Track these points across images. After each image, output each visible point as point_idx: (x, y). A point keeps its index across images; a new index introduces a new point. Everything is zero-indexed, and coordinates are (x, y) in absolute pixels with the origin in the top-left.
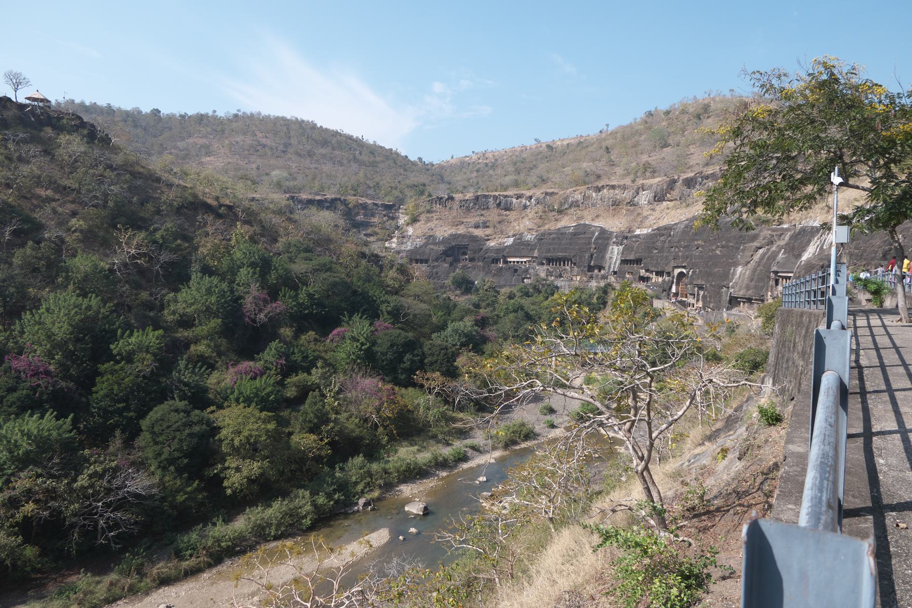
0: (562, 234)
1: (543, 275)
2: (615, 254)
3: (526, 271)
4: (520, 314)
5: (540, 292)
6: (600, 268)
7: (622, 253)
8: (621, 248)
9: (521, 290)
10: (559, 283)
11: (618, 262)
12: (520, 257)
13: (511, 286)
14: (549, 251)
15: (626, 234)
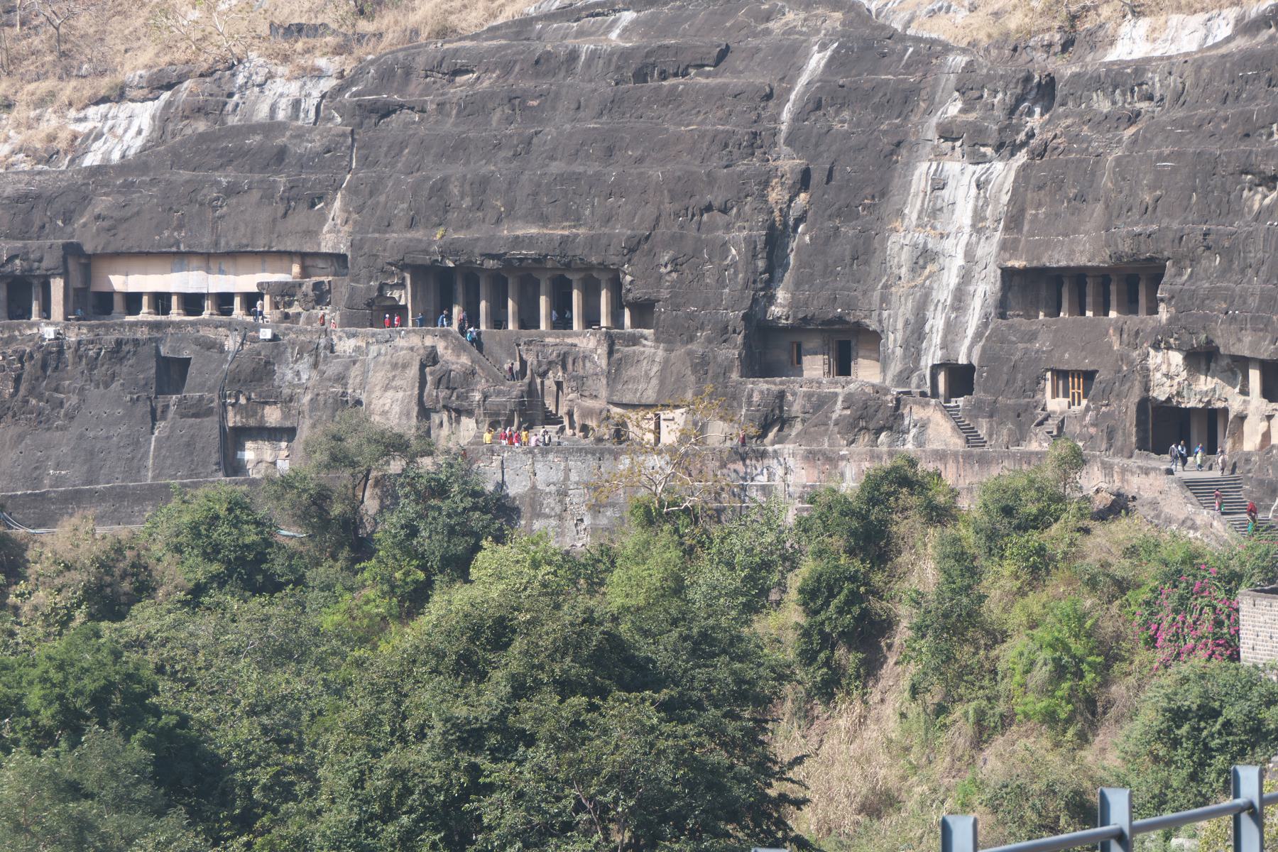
0: (541, 64)
1: (389, 406)
2: (952, 228)
3: (257, 374)
4: (107, 753)
5: (362, 548)
6: (846, 342)
7: (1014, 220)
8: (1003, 172)
9: (200, 535)
10: (518, 470)
11: (985, 288)
12: (213, 258)
13: (122, 501)
14: (436, 204)
15: (1043, 64)
